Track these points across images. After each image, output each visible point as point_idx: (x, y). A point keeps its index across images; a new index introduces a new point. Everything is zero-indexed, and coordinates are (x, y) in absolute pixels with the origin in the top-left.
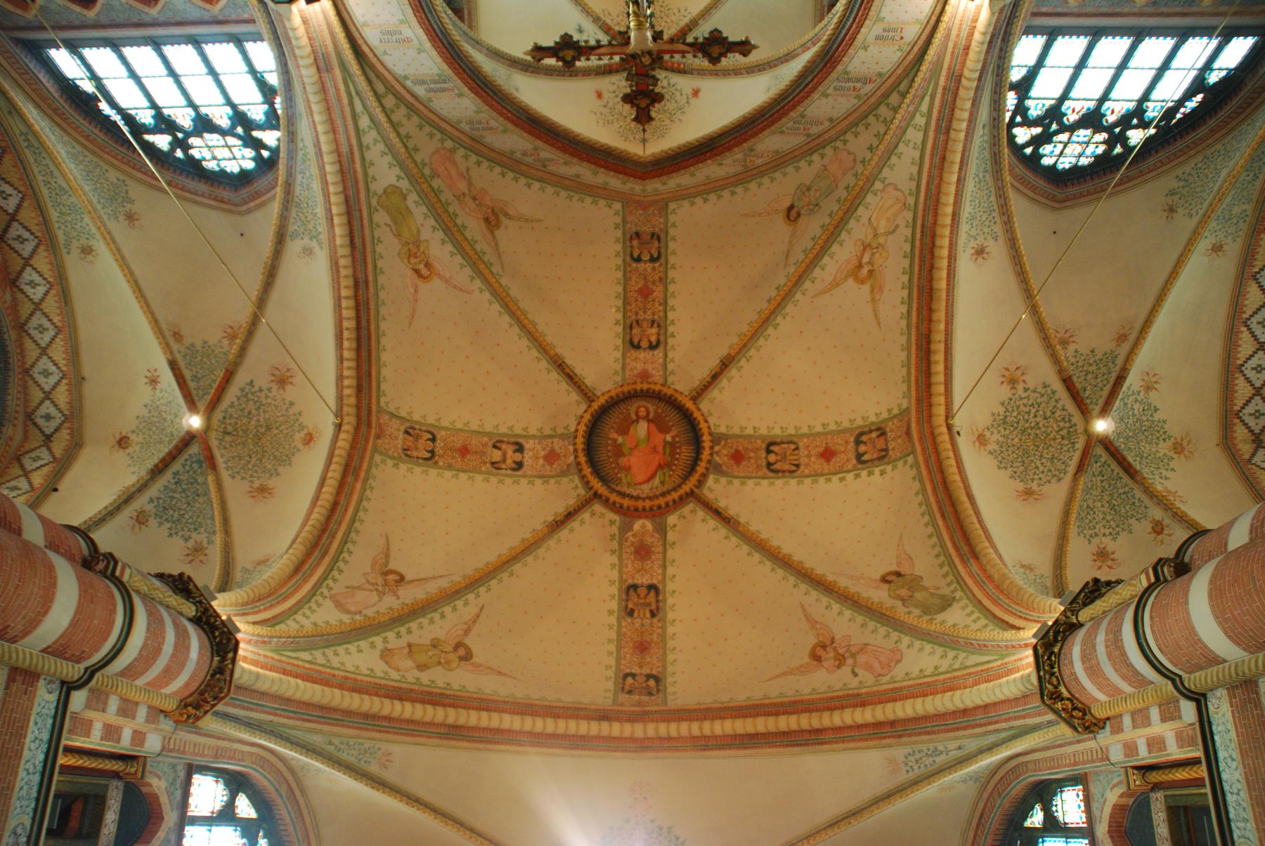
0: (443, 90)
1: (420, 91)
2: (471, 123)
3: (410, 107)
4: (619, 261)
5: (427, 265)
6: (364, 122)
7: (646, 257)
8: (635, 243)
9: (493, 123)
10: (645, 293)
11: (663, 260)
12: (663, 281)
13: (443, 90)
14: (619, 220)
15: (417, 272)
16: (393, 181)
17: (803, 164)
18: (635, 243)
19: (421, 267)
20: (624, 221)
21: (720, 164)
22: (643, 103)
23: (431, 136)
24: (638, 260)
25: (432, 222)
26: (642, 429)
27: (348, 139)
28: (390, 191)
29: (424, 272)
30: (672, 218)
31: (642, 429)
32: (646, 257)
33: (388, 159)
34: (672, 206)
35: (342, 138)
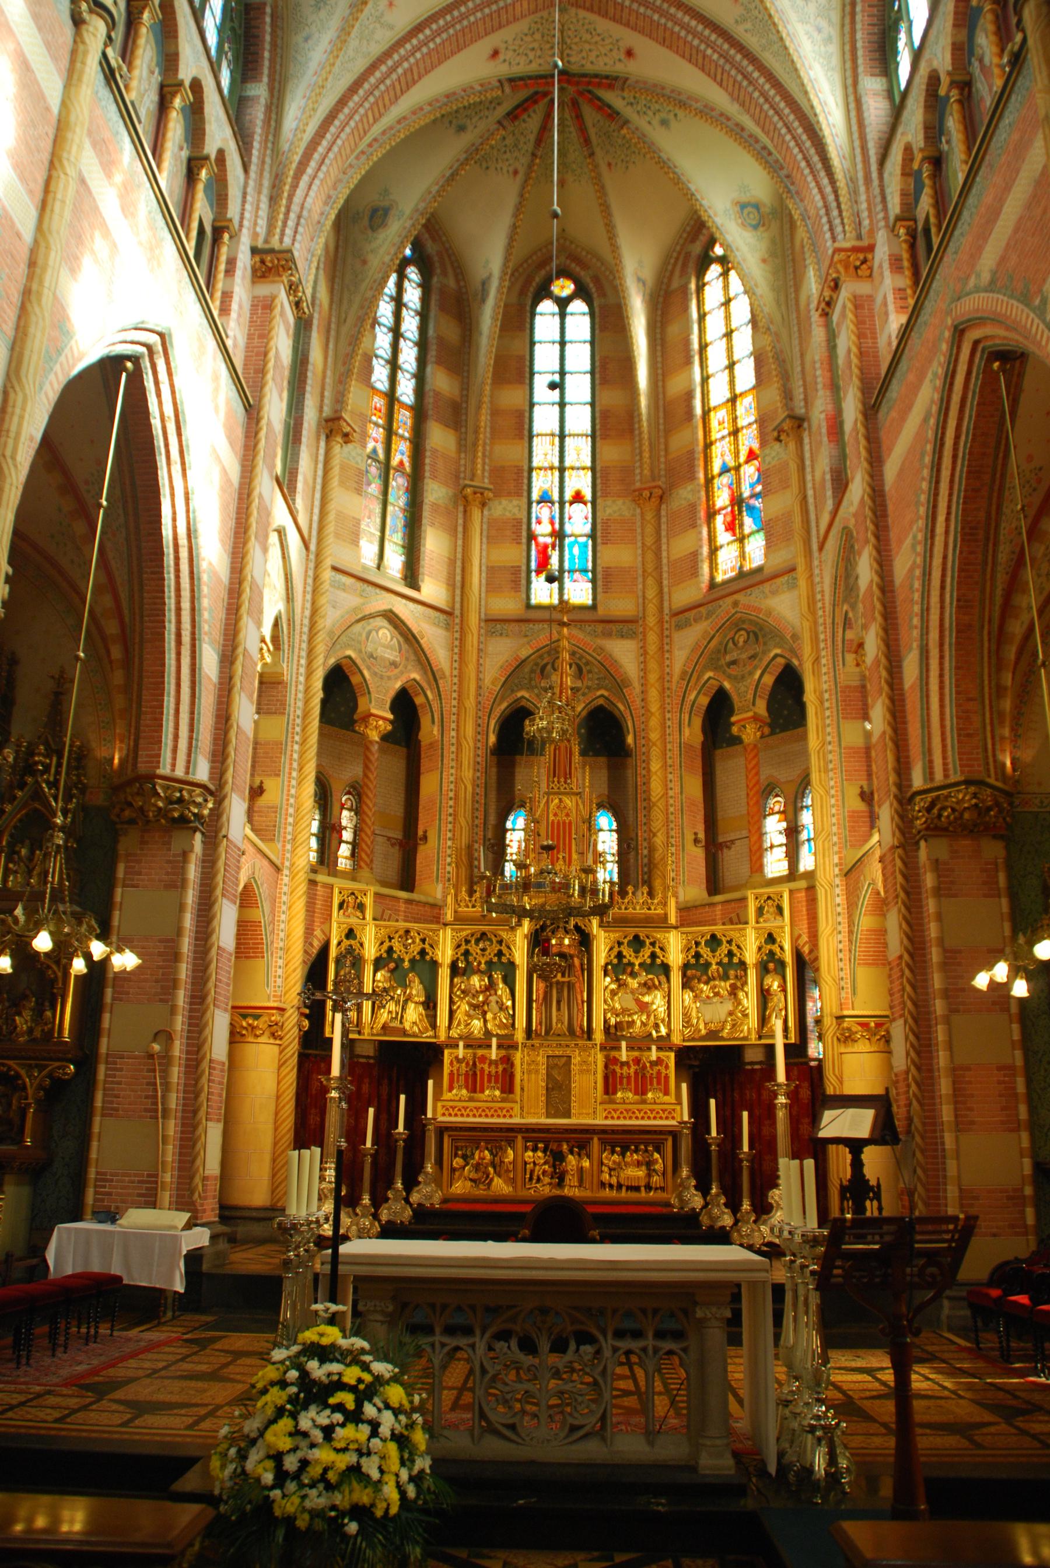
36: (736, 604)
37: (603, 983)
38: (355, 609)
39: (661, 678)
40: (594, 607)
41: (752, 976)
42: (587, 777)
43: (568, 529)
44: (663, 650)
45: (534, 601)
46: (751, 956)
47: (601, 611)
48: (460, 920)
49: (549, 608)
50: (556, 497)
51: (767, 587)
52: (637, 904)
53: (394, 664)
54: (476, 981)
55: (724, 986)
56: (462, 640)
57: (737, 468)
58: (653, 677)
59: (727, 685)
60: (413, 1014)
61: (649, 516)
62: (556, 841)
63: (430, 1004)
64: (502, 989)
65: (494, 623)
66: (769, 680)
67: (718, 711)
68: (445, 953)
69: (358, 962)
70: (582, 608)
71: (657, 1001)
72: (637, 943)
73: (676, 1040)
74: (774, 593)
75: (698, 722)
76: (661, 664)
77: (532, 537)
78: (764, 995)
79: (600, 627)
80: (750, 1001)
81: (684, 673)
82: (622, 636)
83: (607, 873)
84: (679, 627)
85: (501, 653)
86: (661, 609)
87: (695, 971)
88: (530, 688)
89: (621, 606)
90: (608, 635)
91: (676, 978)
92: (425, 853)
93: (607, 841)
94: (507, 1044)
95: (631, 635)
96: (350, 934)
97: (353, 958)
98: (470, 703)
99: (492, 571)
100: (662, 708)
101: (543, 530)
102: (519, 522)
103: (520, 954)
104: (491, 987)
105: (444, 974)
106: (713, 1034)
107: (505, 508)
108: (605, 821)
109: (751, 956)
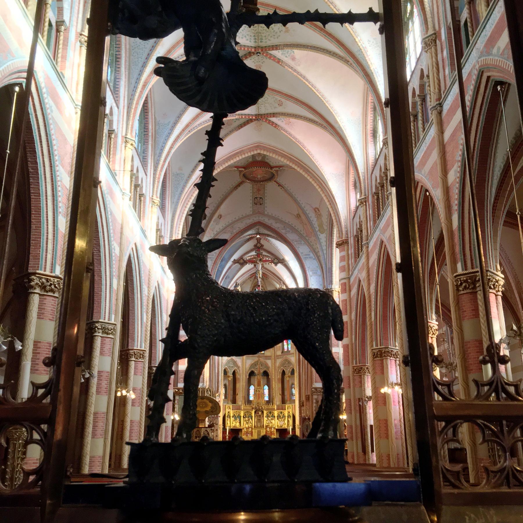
0: (306, 255)
1: (312, 255)
2: (301, 243)
3: (315, 251)
6: (325, 252)
7: (258, 199)
9: (295, 243)
10: (259, 190)
12: (253, 193)
13: (306, 255)
14: (266, 209)
17: (218, 230)
22: (259, 245)
23: (311, 242)
24: (260, 198)
25: (313, 223)
26: (259, 177)
28: (322, 233)
29: (317, 210)
30: (251, 209)
31: (259, 177)
32: (258, 199)
37: (265, 419)
41: (286, 418)
42: (263, 381)
44: (275, 363)
46: (286, 415)
48: (244, 409)
52: (270, 406)
54: (247, 419)
55: (283, 419)
60: (238, 424)
62: (259, 394)
63: (240, 423)
64: (251, 420)
66: (291, 370)
67: (284, 373)
68: (242, 414)
69: (230, 417)
71: (273, 421)
72: (270, 413)
73: (276, 428)
75: (281, 374)
78: (288, 421)
80: (286, 422)
83: (266, 398)
87: (279, 417)
90: (266, 359)
91: (276, 418)
92: (237, 397)
93: (266, 391)
94: (252, 429)
95: (270, 359)
96: (229, 412)
97: (229, 416)
98: (244, 372)
103: (253, 415)
104: (249, 420)
105: (242, 418)
106: (281, 427)
108: (266, 387)
109: (286, 415)
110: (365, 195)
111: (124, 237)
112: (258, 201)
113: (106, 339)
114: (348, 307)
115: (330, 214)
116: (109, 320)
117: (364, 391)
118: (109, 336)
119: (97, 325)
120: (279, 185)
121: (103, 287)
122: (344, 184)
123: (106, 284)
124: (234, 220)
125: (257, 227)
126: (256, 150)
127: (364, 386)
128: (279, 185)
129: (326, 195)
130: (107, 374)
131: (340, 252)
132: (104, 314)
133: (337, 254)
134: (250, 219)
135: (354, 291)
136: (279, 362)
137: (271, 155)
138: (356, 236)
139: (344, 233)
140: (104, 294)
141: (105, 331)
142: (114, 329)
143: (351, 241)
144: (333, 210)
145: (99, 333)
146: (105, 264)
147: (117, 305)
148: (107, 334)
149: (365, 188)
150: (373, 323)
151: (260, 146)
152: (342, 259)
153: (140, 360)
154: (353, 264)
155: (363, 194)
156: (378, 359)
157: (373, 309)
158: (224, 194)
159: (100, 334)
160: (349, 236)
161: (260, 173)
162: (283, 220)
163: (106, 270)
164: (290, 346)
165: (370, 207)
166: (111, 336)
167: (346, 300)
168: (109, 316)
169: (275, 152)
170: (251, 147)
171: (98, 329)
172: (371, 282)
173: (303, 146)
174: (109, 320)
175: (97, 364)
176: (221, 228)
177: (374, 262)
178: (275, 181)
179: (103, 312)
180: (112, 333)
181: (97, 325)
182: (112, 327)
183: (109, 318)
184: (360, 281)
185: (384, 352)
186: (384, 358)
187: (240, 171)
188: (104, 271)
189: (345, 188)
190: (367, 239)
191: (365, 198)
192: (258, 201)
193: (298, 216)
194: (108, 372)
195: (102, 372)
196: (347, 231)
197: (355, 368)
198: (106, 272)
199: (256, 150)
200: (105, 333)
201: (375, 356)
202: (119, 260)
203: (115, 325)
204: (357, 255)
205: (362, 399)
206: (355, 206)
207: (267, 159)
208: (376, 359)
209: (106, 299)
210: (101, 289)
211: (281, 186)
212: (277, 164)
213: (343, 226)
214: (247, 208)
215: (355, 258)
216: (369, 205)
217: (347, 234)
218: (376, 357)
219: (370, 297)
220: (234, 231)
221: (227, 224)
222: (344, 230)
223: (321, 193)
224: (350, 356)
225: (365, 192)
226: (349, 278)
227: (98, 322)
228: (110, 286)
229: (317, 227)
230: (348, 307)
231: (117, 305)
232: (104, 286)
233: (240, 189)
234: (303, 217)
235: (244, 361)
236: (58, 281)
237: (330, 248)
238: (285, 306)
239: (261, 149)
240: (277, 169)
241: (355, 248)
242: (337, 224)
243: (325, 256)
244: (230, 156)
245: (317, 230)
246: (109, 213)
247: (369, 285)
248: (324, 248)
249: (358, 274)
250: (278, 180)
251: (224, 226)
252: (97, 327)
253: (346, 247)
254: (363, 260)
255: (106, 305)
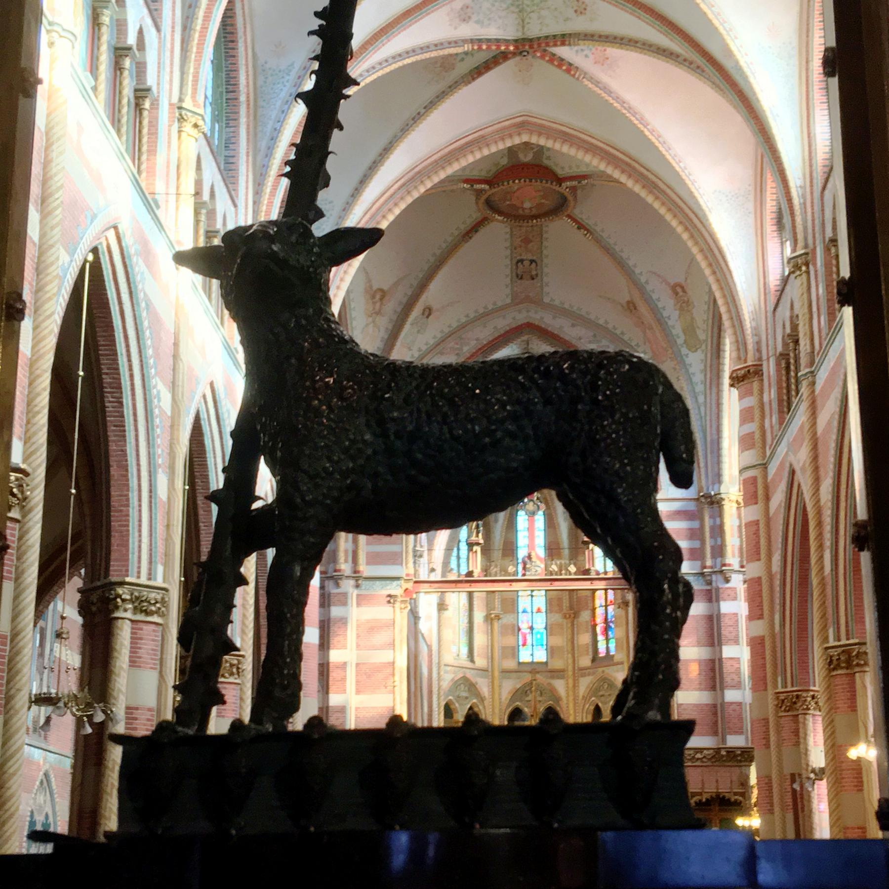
4: (545, 261)
5: (677, 294)
7: (527, 263)
8: (534, 273)
10: (527, 241)
11: (514, 262)
12: (513, 248)
14: (546, 289)
15: (684, 291)
16: (691, 354)
17: (424, 348)
18: (534, 273)
19: (681, 294)
20: (542, 287)
21: (477, 339)
24: (532, 261)
25: (670, 323)
26: (527, 205)
27: (711, 394)
28: (693, 348)
29: (679, 290)
30: (508, 291)
31: (527, 205)
32: (527, 263)
33: (691, 370)
34: (509, 301)
35: (714, 395)
36: (603, 672)
38: (453, 679)
39: (574, 699)
40: (546, 663)
43: (534, 626)
44: (575, 686)
45: (521, 661)
47: (550, 667)
49: (528, 663)
50: (529, 610)
51: (615, 668)
53: (467, 698)
56: (493, 682)
57: (606, 606)
58: (571, 698)
59: (600, 705)
61: (569, 625)
65: (505, 672)
70: (541, 663)
74: (618, 671)
76: (574, 692)
77: (519, 629)
79: (549, 674)
81: (583, 697)
82: (558, 678)
84: (583, 675)
85: (508, 687)
86: (574, 668)
88: (521, 701)
89: (558, 664)
90: (552, 677)
95: (562, 677)
98: (497, 711)
99: (504, 648)
100: (575, 711)
101: (524, 627)
102: (513, 626)
107: (507, 619)
110: (806, 246)
111: (183, 367)
112: (526, 270)
113: (145, 627)
114: (763, 542)
115: (715, 301)
116: (149, 579)
117: (806, 754)
118: (150, 619)
119: (120, 591)
120: (581, 226)
121: (133, 496)
122: (751, 219)
123: (139, 486)
124: (464, 320)
125: (525, 338)
126: (519, 134)
127: (806, 744)
128: (581, 226)
129: (702, 251)
130: (148, 715)
131: (741, 398)
132: (136, 565)
133: (732, 402)
134: (504, 317)
135: (778, 498)
136: (585, 683)
137: (557, 146)
138: (781, 354)
139: (750, 347)
140: (136, 514)
141: (141, 606)
142: (163, 602)
143: (770, 368)
144: (722, 289)
145: (126, 610)
146: (137, 436)
147: (168, 539)
148: (147, 613)
149: (805, 228)
150: (829, 581)
151: (529, 123)
152: (746, 416)
153: (231, 680)
154: (776, 427)
155: (801, 244)
156: (839, 672)
157: (828, 543)
158: (438, 252)
159: (129, 615)
160: (765, 357)
161: (528, 195)
162: (592, 317)
163: (137, 451)
164: (612, 645)
165: (820, 279)
166: (155, 619)
167: (757, 523)
168: (150, 569)
169: (566, 138)
170: (504, 128)
171: (123, 600)
172: (822, 472)
173: (642, 120)
174: (149, 579)
175: (124, 689)
176: (432, 342)
177: (829, 423)
178: (569, 216)
179: (133, 558)
180: (157, 612)
181: (120, 591)
182: (159, 597)
183: (150, 574)
184: (793, 473)
185: (857, 656)
186: (857, 669)
187: (479, 192)
188: (134, 453)
189: (752, 231)
190: (812, 363)
191: (807, 254)
192: (526, 270)
193: (631, 307)
194: (150, 710)
195: (137, 709)
196: (758, 343)
197: (782, 697)
198: (138, 455)
199: (519, 134)
200: (142, 611)
201: (832, 664)
202: (172, 426)
203: (166, 590)
204: (786, 405)
205: (800, 775)
206: (779, 277)
207: (549, 158)
208: (834, 673)
209: (140, 526)
210: (128, 500)
211: (586, 229)
212: (575, 171)
213: (749, 331)
214: (498, 289)
215: (781, 412)
216: (816, 271)
217: (759, 350)
218: (834, 669)
219: (819, 513)
220: (465, 349)
221: (447, 330)
222: (750, 340)
223: (690, 243)
224: (768, 666)
225: (806, 239)
226: (764, 466)
227: (122, 584)
228: (151, 491)
229: (681, 335)
230: (763, 542)
231: (168, 539)
232: (136, 493)
233: (477, 237)
234: (643, 309)
235: (496, 683)
236: (17, 479)
237: (714, 390)
238: (536, 397)
239: (531, 132)
240: (574, 183)
241: (780, 388)
242: (734, 326)
243: (702, 409)
244: (450, 153)
245: (680, 341)
246: (143, 305)
247: (817, 481)
248: (699, 388)
249: (787, 453)
250: (577, 212)
251: (439, 335)
252: (120, 596)
253: (756, 385)
254: (801, 417)
255: (140, 541)
